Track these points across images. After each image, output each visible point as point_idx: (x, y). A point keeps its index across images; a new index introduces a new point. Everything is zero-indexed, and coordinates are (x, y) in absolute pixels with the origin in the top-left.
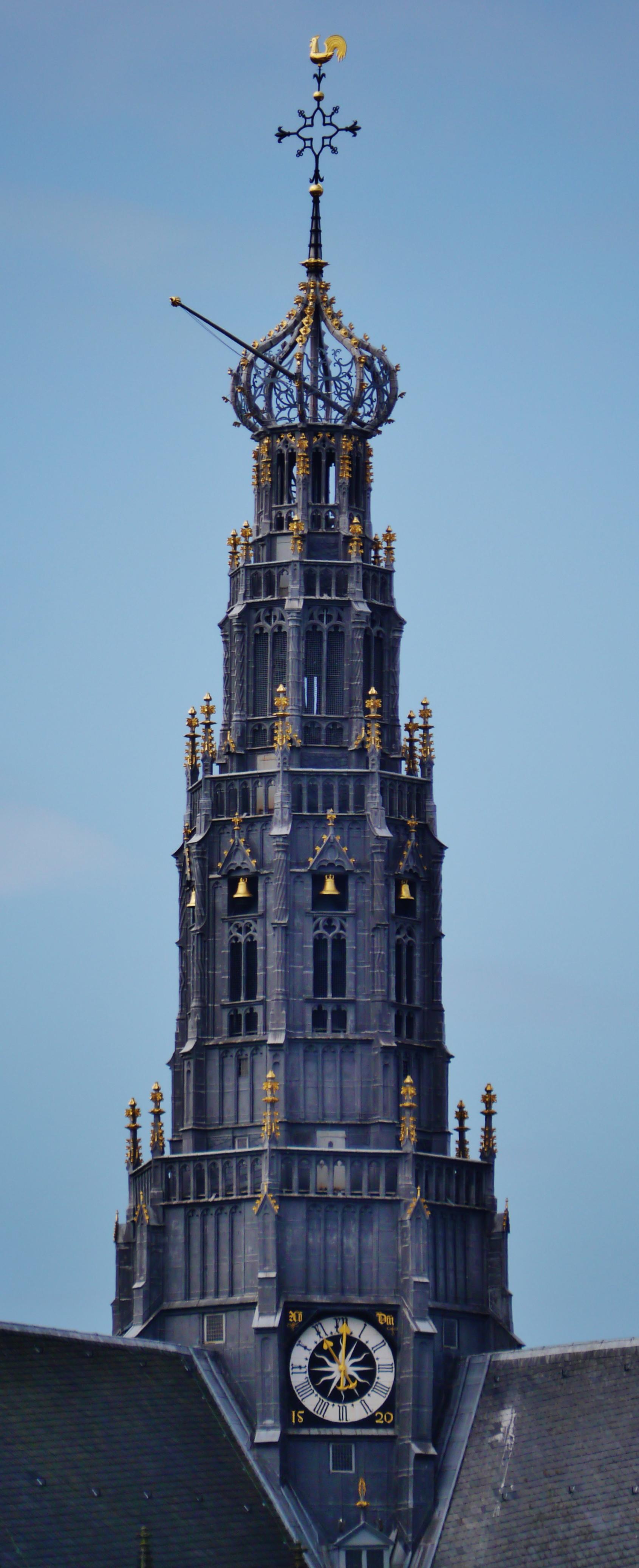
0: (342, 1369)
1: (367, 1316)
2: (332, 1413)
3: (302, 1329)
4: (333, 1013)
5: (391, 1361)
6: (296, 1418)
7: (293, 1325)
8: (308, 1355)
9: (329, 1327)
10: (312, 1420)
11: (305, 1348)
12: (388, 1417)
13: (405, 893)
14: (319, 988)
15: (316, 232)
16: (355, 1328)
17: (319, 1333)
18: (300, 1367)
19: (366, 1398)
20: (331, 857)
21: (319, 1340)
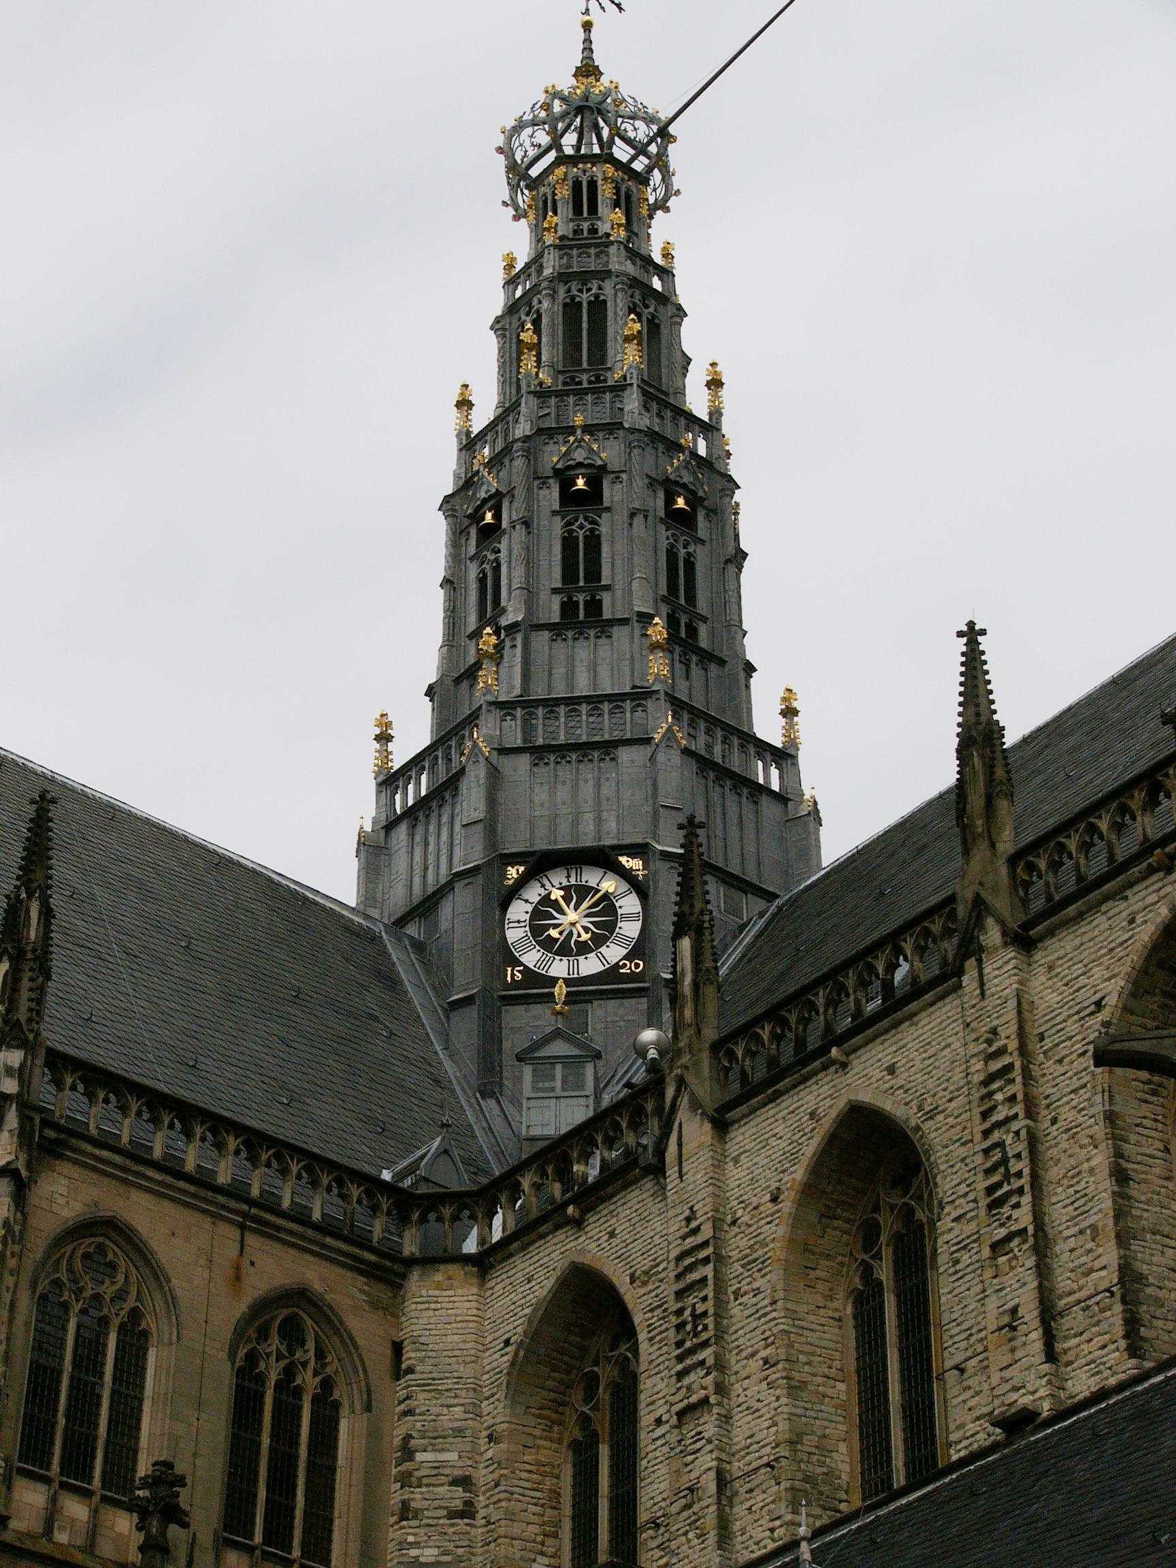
0: (574, 919)
1: (604, 859)
2: (559, 968)
3: (522, 882)
4: (586, 602)
5: (639, 909)
6: (513, 975)
7: (511, 882)
8: (530, 908)
10: (533, 978)
11: (527, 901)
12: (637, 966)
13: (681, 503)
16: (591, 877)
17: (543, 886)
18: (519, 922)
19: (603, 949)
20: (579, 455)
21: (543, 893)
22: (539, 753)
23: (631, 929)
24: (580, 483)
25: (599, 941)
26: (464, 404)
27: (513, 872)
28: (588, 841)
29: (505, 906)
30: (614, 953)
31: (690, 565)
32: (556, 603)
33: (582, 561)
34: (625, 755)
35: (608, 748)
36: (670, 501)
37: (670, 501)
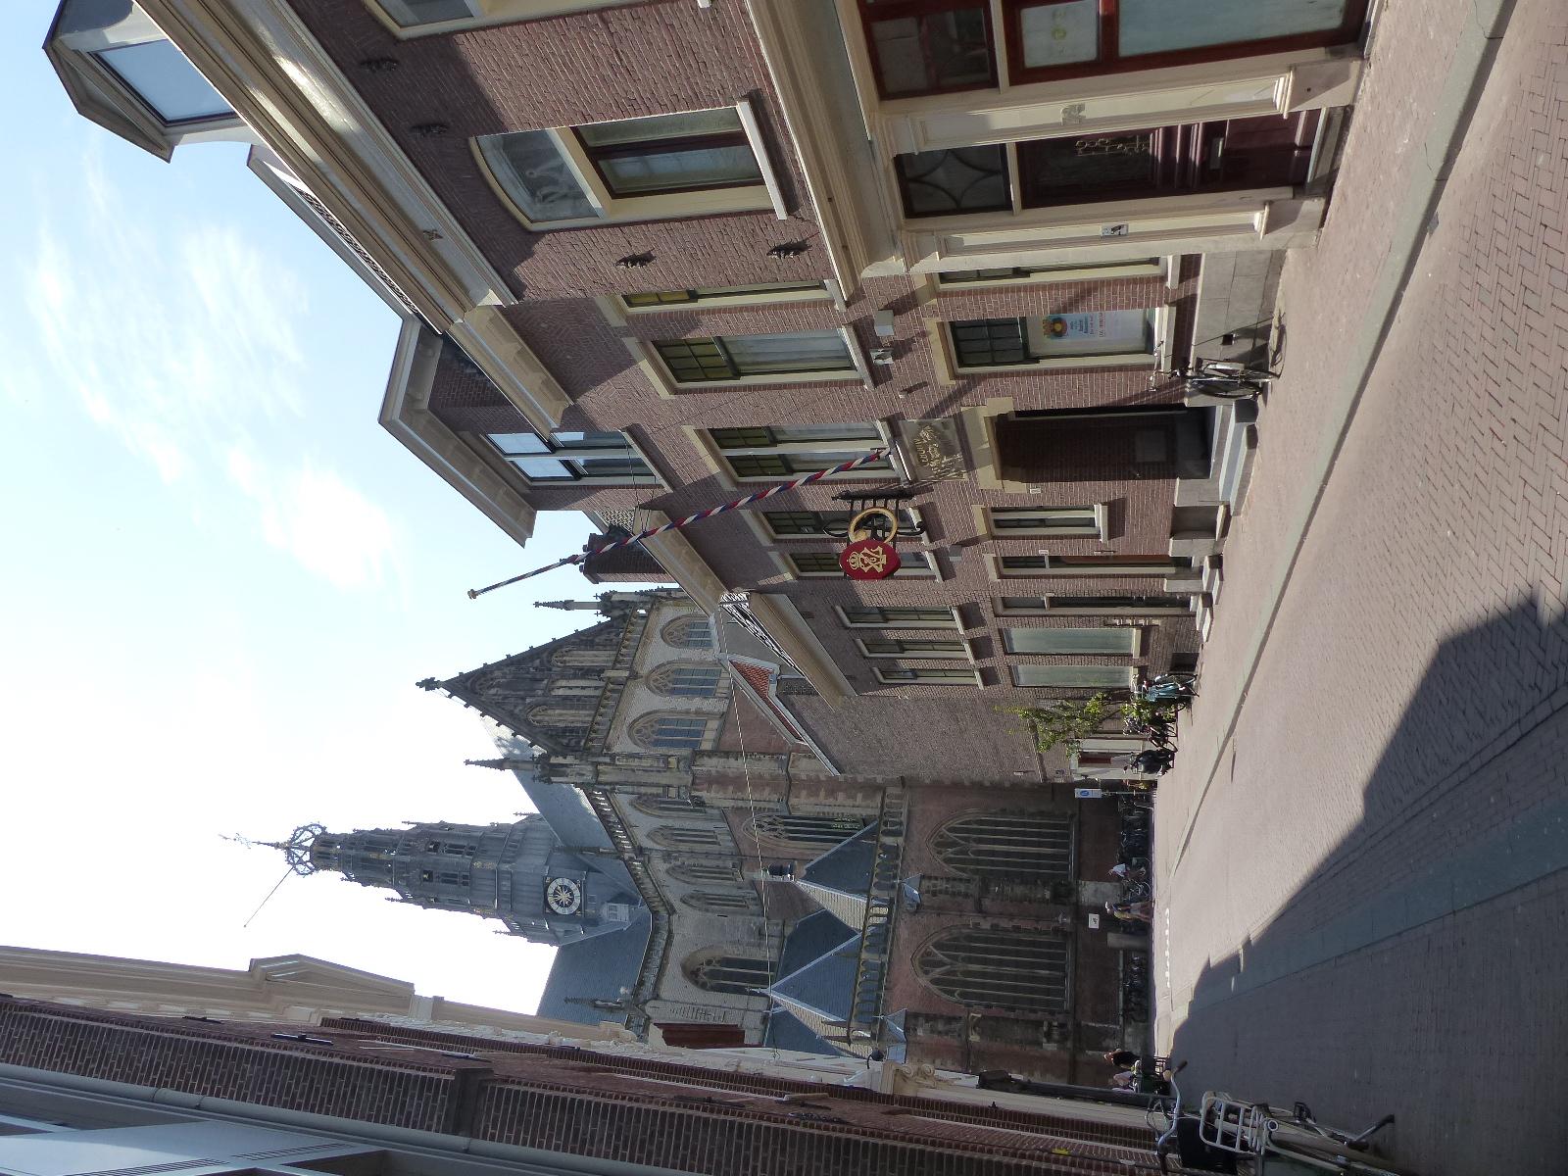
0: (564, 896)
1: (548, 886)
2: (577, 901)
3: (550, 908)
9: (550, 899)
10: (579, 909)
13: (431, 847)
14: (455, 882)
15: (268, 844)
16: (550, 891)
23: (566, 882)
25: (570, 890)
26: (393, 900)
30: (573, 886)
31: (451, 846)
36: (430, 850)
37: (430, 850)
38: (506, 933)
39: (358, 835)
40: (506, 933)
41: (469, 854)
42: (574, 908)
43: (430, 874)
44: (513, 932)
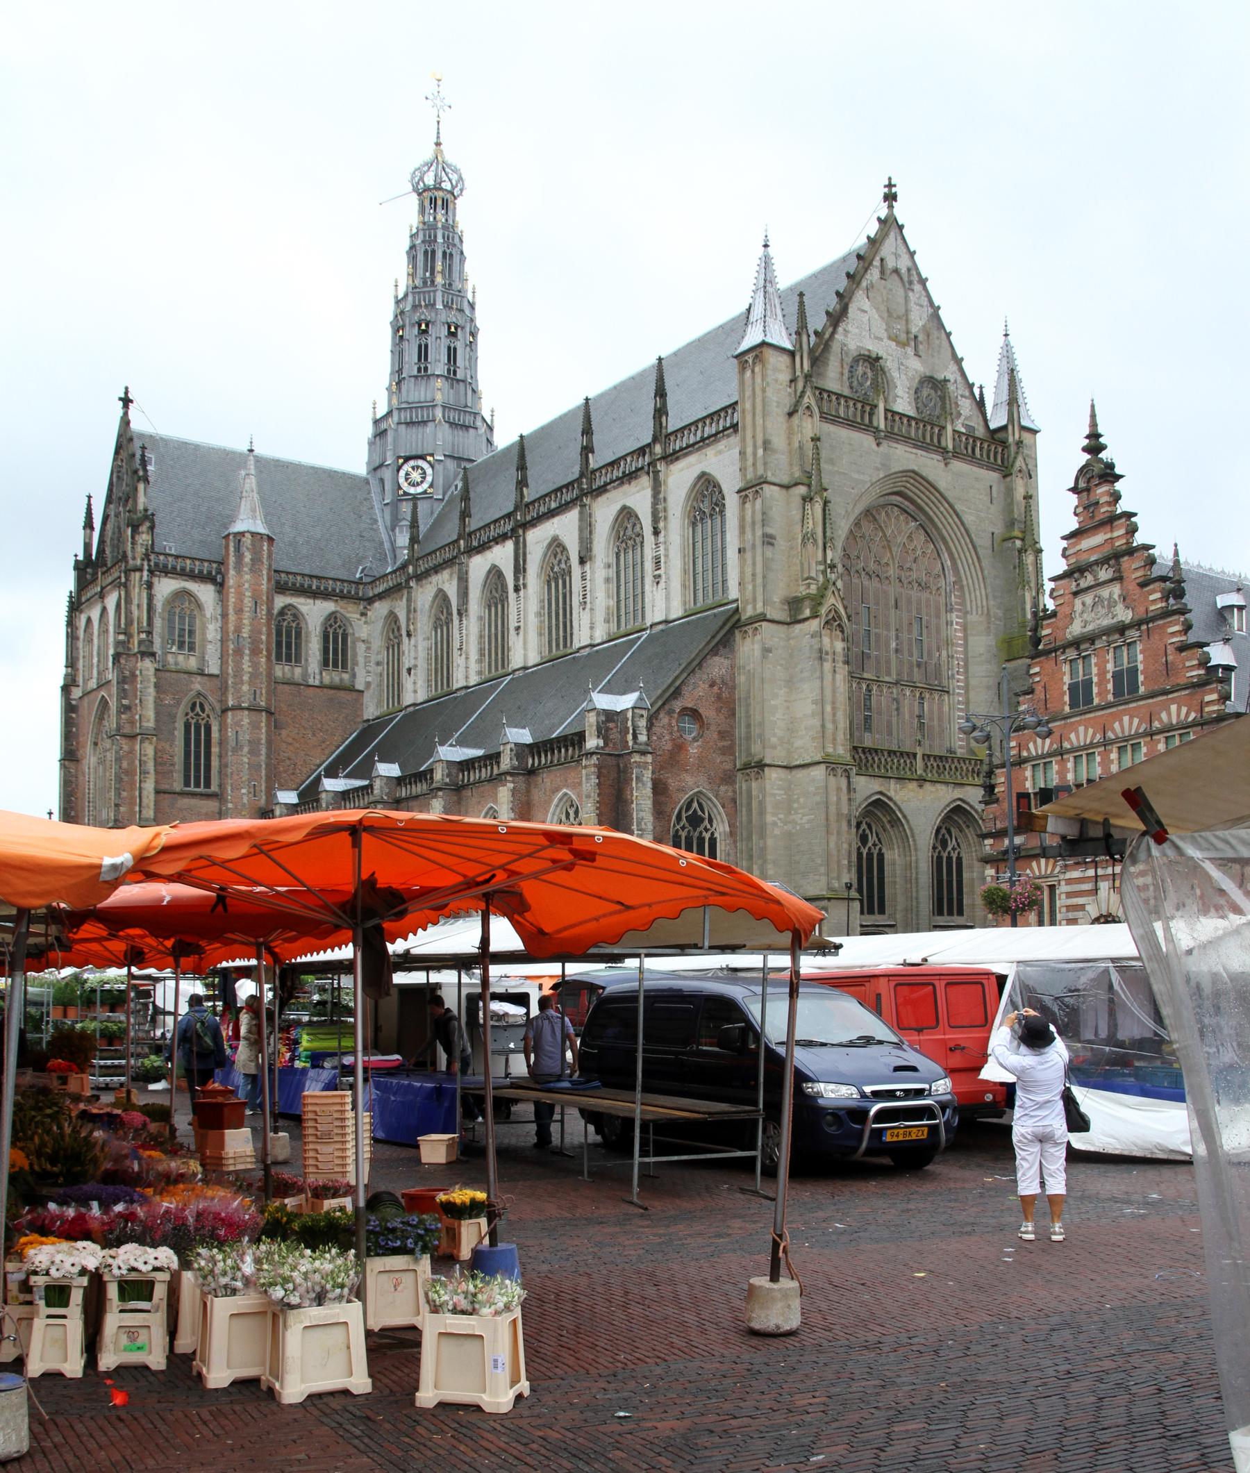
0: (416, 476)
1: (423, 457)
2: (412, 490)
9: (412, 463)
10: (406, 494)
13: (453, 329)
14: (420, 359)
16: (420, 463)
22: (407, 424)
23: (429, 479)
24: (423, 327)
27: (401, 461)
28: (419, 453)
29: (398, 471)
30: (425, 486)
31: (455, 349)
32: (416, 368)
33: (423, 353)
34: (430, 424)
35: (424, 423)
37: (449, 328)
38: (375, 413)
39: (457, 241)
40: (375, 413)
41: (449, 370)
42: (405, 486)
43: (425, 332)
44: (376, 422)
